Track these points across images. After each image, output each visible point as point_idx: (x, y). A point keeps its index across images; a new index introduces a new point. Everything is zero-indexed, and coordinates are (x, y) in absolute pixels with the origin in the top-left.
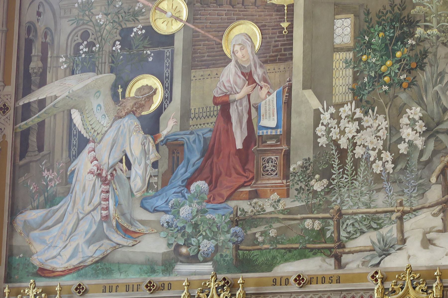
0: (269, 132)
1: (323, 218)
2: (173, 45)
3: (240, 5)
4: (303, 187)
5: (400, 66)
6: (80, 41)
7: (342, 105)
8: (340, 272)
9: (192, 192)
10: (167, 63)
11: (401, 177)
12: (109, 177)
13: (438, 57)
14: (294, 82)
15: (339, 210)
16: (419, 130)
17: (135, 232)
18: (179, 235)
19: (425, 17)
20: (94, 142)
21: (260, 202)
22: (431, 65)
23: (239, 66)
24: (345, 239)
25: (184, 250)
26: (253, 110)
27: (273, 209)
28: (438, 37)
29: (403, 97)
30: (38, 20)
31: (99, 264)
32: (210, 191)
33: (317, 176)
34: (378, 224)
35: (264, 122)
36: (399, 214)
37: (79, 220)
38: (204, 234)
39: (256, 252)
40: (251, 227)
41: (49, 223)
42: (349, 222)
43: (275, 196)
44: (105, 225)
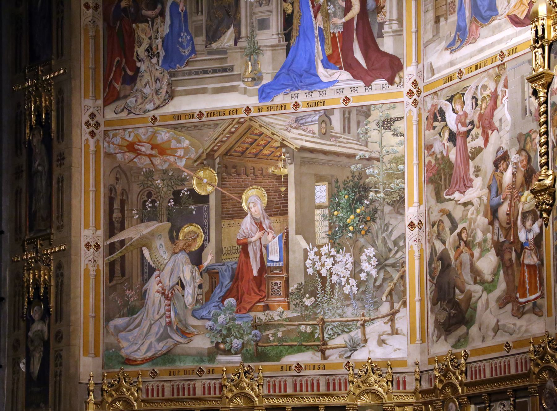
0: (275, 264)
1: (312, 325)
2: (209, 202)
3: (252, 175)
4: (299, 303)
5: (360, 219)
6: (146, 199)
7: (322, 246)
8: (325, 362)
9: (226, 306)
10: (205, 215)
11: (363, 296)
12: (170, 295)
13: (384, 213)
14: (290, 229)
15: (323, 319)
16: (373, 264)
17: (189, 334)
18: (218, 336)
19: (375, 184)
20: (159, 270)
21: (271, 313)
22: (380, 219)
23: (254, 218)
24: (327, 339)
25: (222, 346)
26: (264, 249)
27: (279, 318)
28: (384, 199)
29: (362, 240)
30: (117, 183)
31: (166, 356)
32: (237, 305)
33: (307, 295)
34: (348, 329)
35: (271, 258)
36: (362, 322)
37: (151, 325)
38: (235, 335)
39: (269, 348)
40: (265, 330)
41: (131, 327)
42: (330, 327)
43: (280, 309)
44: (169, 328)
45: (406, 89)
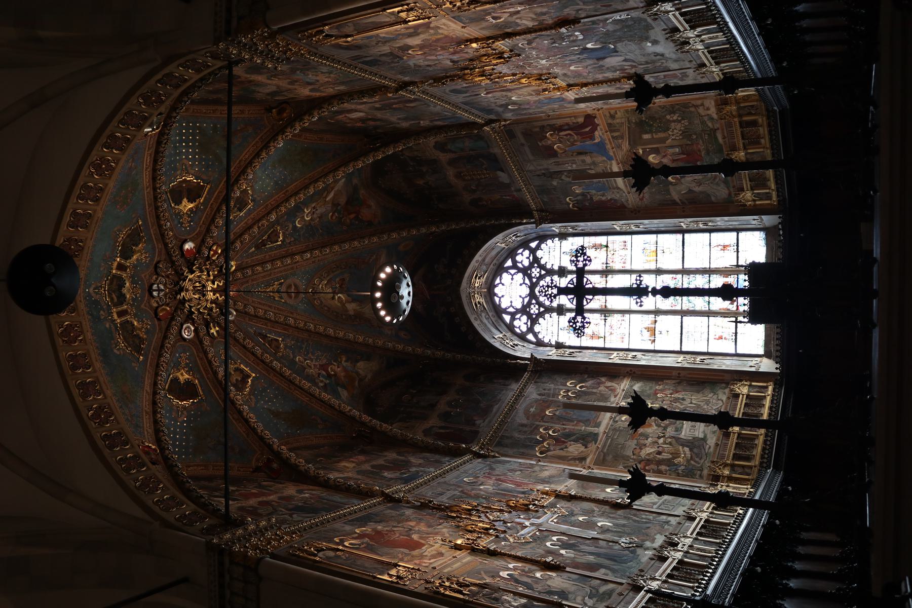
29: (664, 120)
45: (597, 112)
